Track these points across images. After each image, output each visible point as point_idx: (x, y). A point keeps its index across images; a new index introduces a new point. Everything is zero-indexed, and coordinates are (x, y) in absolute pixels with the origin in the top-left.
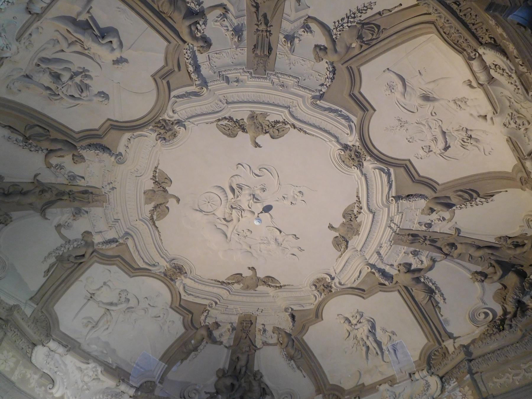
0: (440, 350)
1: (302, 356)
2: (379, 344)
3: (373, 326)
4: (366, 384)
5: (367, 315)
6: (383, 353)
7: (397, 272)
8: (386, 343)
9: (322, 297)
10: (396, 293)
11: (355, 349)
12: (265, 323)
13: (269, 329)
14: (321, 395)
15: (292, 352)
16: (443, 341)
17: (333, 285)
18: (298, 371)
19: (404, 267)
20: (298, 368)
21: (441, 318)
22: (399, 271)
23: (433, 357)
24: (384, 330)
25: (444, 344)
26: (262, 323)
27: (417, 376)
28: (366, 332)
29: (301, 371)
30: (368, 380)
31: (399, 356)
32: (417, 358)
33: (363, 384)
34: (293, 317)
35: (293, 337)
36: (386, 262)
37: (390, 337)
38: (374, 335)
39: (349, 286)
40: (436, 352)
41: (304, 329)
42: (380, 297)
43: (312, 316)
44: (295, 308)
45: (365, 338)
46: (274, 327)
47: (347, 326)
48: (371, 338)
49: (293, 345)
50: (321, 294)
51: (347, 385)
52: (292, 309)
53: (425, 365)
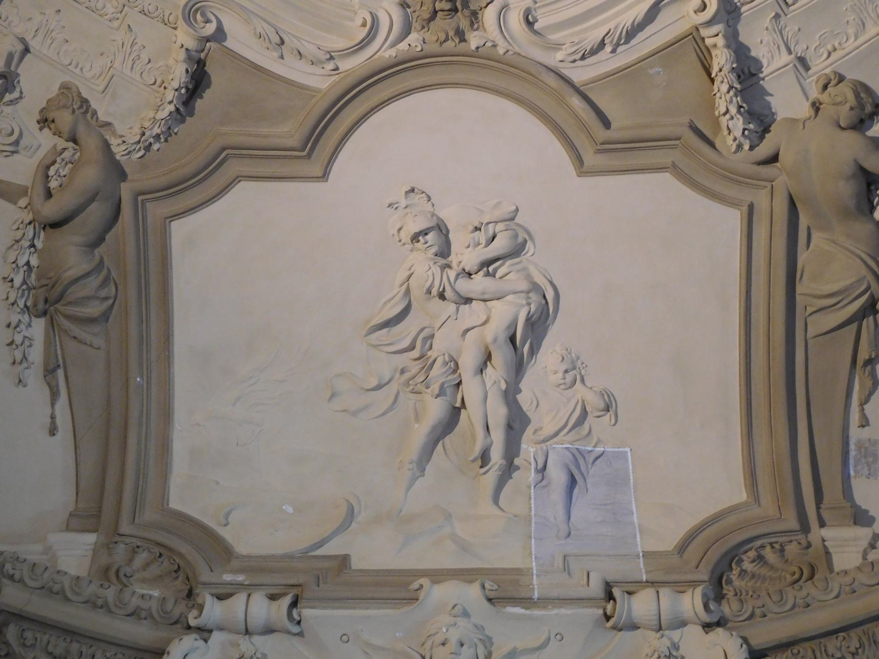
0: (792, 549)
1: (105, 316)
2: (517, 424)
3: (538, 324)
4: (356, 564)
5: (538, 261)
6: (509, 468)
7: (804, 110)
8: (549, 430)
9: (403, 46)
10: (734, 219)
11: (385, 397)
12: (33, 44)
13: (37, 84)
14: (92, 538)
15: (73, 260)
16: (822, 524)
17: (489, 16)
18: (36, 387)
19: (857, 95)
20: (49, 371)
21: (856, 433)
22: (816, 107)
23: (747, 565)
24: (574, 372)
25: (825, 532)
26: (19, 30)
27: (642, 605)
28: (496, 329)
29: (54, 395)
30: (372, 551)
31: (577, 512)
32: (668, 542)
33: (344, 561)
34: (198, 81)
35: (126, 190)
36: (790, 31)
37: (584, 413)
38: (519, 368)
39: (554, 59)
40: (768, 553)
41: (201, 180)
42: (653, 197)
43: (288, 132)
44: (242, 39)
45: (468, 361)
46: (65, 87)
47: (422, 265)
48: (496, 375)
49: (100, 240)
50: (406, 31)
51: (250, 538)
52: (220, 35)
53: (703, 574)
